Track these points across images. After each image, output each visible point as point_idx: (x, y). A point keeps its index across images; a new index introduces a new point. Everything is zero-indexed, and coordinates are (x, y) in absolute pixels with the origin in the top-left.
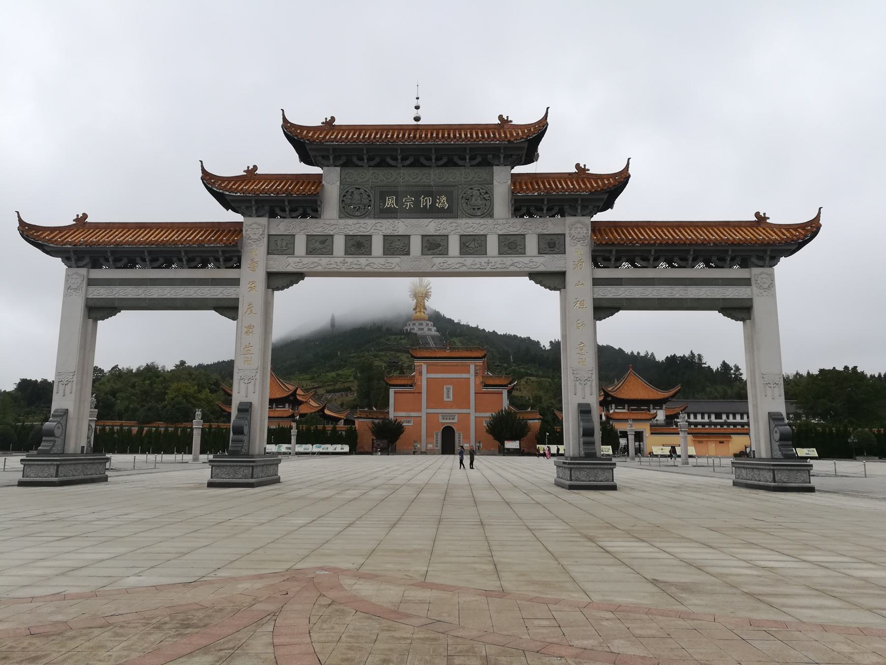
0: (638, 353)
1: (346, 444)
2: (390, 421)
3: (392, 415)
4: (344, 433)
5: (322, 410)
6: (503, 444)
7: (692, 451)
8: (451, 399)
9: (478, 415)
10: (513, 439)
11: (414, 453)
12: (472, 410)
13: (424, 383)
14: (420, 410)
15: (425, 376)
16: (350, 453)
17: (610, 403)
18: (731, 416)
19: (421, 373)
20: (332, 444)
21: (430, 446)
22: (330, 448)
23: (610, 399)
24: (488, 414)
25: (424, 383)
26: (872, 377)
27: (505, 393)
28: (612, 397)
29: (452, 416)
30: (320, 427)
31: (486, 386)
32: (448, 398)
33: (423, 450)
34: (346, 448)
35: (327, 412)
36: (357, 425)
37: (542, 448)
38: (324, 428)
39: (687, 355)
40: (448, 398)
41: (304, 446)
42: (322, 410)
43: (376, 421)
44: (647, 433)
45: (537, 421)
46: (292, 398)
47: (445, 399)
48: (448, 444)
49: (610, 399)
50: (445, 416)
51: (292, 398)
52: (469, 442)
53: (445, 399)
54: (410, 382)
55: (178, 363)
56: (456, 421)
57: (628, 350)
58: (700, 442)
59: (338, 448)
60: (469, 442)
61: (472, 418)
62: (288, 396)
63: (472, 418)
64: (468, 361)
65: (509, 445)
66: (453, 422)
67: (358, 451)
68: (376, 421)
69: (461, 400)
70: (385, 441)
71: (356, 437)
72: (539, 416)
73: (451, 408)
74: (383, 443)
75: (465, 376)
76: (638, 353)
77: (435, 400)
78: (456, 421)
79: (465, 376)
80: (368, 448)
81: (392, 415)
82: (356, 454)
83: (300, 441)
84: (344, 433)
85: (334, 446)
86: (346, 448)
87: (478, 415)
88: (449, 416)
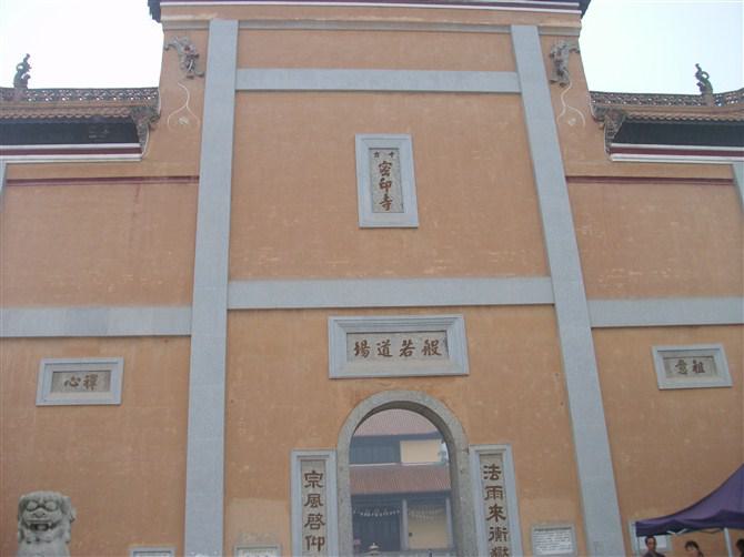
8: (409, 215)
12: (566, 281)
47: (368, 215)
53: (368, 215)
61: (575, 335)
78: (456, 358)
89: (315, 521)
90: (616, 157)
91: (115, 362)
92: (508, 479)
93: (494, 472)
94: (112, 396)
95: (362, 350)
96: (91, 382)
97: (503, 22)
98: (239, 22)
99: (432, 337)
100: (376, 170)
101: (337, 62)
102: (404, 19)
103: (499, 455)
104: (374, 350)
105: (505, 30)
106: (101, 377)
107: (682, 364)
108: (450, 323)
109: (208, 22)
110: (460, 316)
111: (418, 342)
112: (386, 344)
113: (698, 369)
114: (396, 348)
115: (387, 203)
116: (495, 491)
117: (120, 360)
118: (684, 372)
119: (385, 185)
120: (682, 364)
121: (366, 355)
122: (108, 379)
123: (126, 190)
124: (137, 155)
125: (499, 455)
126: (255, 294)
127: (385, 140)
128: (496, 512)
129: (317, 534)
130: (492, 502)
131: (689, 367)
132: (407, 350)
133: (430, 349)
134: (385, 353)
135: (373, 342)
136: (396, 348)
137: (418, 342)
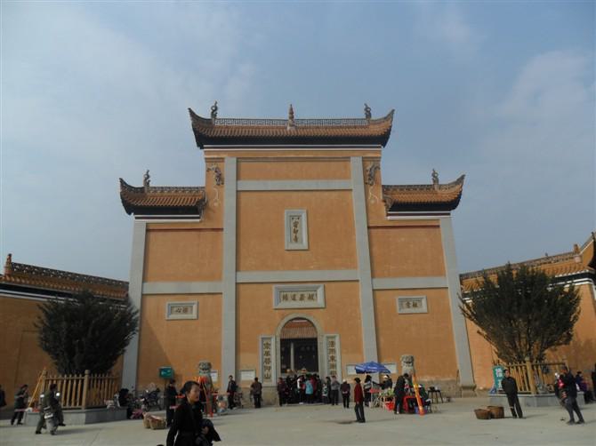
8: (304, 245)
9: (380, 283)
12: (361, 272)
14: (215, 276)
29: (307, 290)
31: (397, 207)
56: (320, 301)
63: (364, 294)
89: (268, 361)
90: (389, 218)
91: (194, 301)
92: (337, 347)
93: (333, 344)
94: (194, 315)
95: (285, 298)
96: (185, 311)
97: (344, 156)
98: (238, 159)
99: (311, 293)
100: (292, 225)
101: (277, 177)
102: (306, 156)
103: (334, 337)
104: (290, 298)
105: (347, 159)
106: (189, 309)
107: (408, 304)
108: (318, 288)
109: (223, 159)
110: (322, 285)
111: (306, 295)
112: (294, 295)
113: (415, 305)
114: (298, 297)
115: (296, 239)
117: (196, 302)
118: (409, 307)
119: (296, 232)
120: (408, 304)
121: (287, 299)
122: (192, 310)
124: (198, 220)
125: (334, 337)
127: (296, 211)
128: (333, 358)
129: (268, 365)
130: (331, 355)
131: (411, 305)
132: (302, 298)
133: (311, 298)
134: (294, 299)
135: (289, 294)
136: (298, 297)
137: (306, 295)
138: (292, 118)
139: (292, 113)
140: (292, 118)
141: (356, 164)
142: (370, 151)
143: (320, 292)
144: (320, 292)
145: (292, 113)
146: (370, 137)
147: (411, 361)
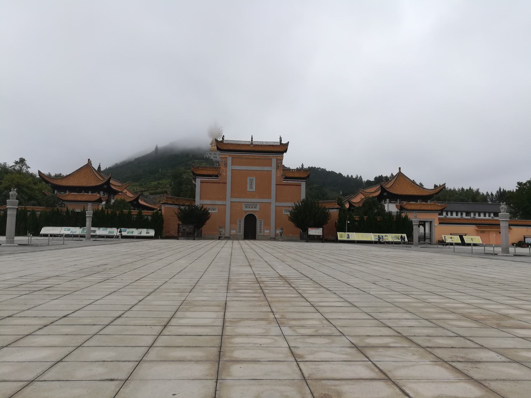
0: (352, 176)
1: (151, 228)
2: (196, 208)
3: (198, 202)
4: (150, 218)
5: (137, 200)
6: (307, 231)
7: (477, 240)
8: (254, 190)
9: (278, 204)
10: (316, 226)
11: (220, 238)
12: (273, 200)
13: (229, 173)
14: (224, 199)
15: (230, 167)
16: (155, 237)
17: (385, 198)
18: (449, 214)
19: (226, 165)
20: (137, 228)
21: (233, 232)
22: (136, 232)
23: (385, 194)
24: (291, 204)
25: (229, 173)
26: (508, 192)
27: (303, 184)
28: (388, 193)
29: (254, 205)
30: (126, 211)
31: (287, 178)
32: (251, 187)
33: (227, 235)
34: (152, 233)
35: (141, 202)
36: (163, 211)
37: (342, 236)
38: (130, 212)
39: (389, 176)
40: (251, 187)
41: (109, 229)
42: (137, 200)
43: (183, 208)
44: (436, 223)
45: (335, 210)
46: (105, 187)
47: (249, 190)
48: (250, 231)
49: (385, 194)
50: (248, 205)
51: (105, 187)
52: (270, 229)
53: (249, 190)
54: (215, 173)
55: (18, 160)
57: (345, 174)
58: (482, 232)
59: (144, 232)
60: (270, 229)
61: (273, 207)
62: (102, 185)
63: (273, 207)
64: (270, 156)
65: (312, 232)
66: (255, 210)
67: (164, 235)
68: (183, 208)
69: (263, 190)
70: (191, 226)
71: (162, 221)
72: (337, 206)
73: (253, 198)
74: (189, 228)
75: (266, 168)
76: (352, 176)
77: (239, 189)
78: (257, 209)
79: (266, 168)
80: (174, 233)
81: (198, 202)
82: (162, 238)
83: (95, 224)
84: (150, 218)
85: (140, 230)
86: (152, 233)
87: (278, 204)
88: (251, 204)
89: (240, 227)
92: (262, 224)
95: (246, 207)
96: (214, 210)
105: (271, 159)
111: (253, 206)
116: (261, 225)
123: (217, 184)
126: (234, 200)
132: (252, 207)
133: (255, 207)
137: (253, 206)
138: (252, 140)
139: (252, 139)
140: (252, 140)
141: (274, 161)
142: (278, 156)
143: (258, 206)
144: (258, 206)
145: (252, 139)
146: (281, 149)
147: (282, 229)
